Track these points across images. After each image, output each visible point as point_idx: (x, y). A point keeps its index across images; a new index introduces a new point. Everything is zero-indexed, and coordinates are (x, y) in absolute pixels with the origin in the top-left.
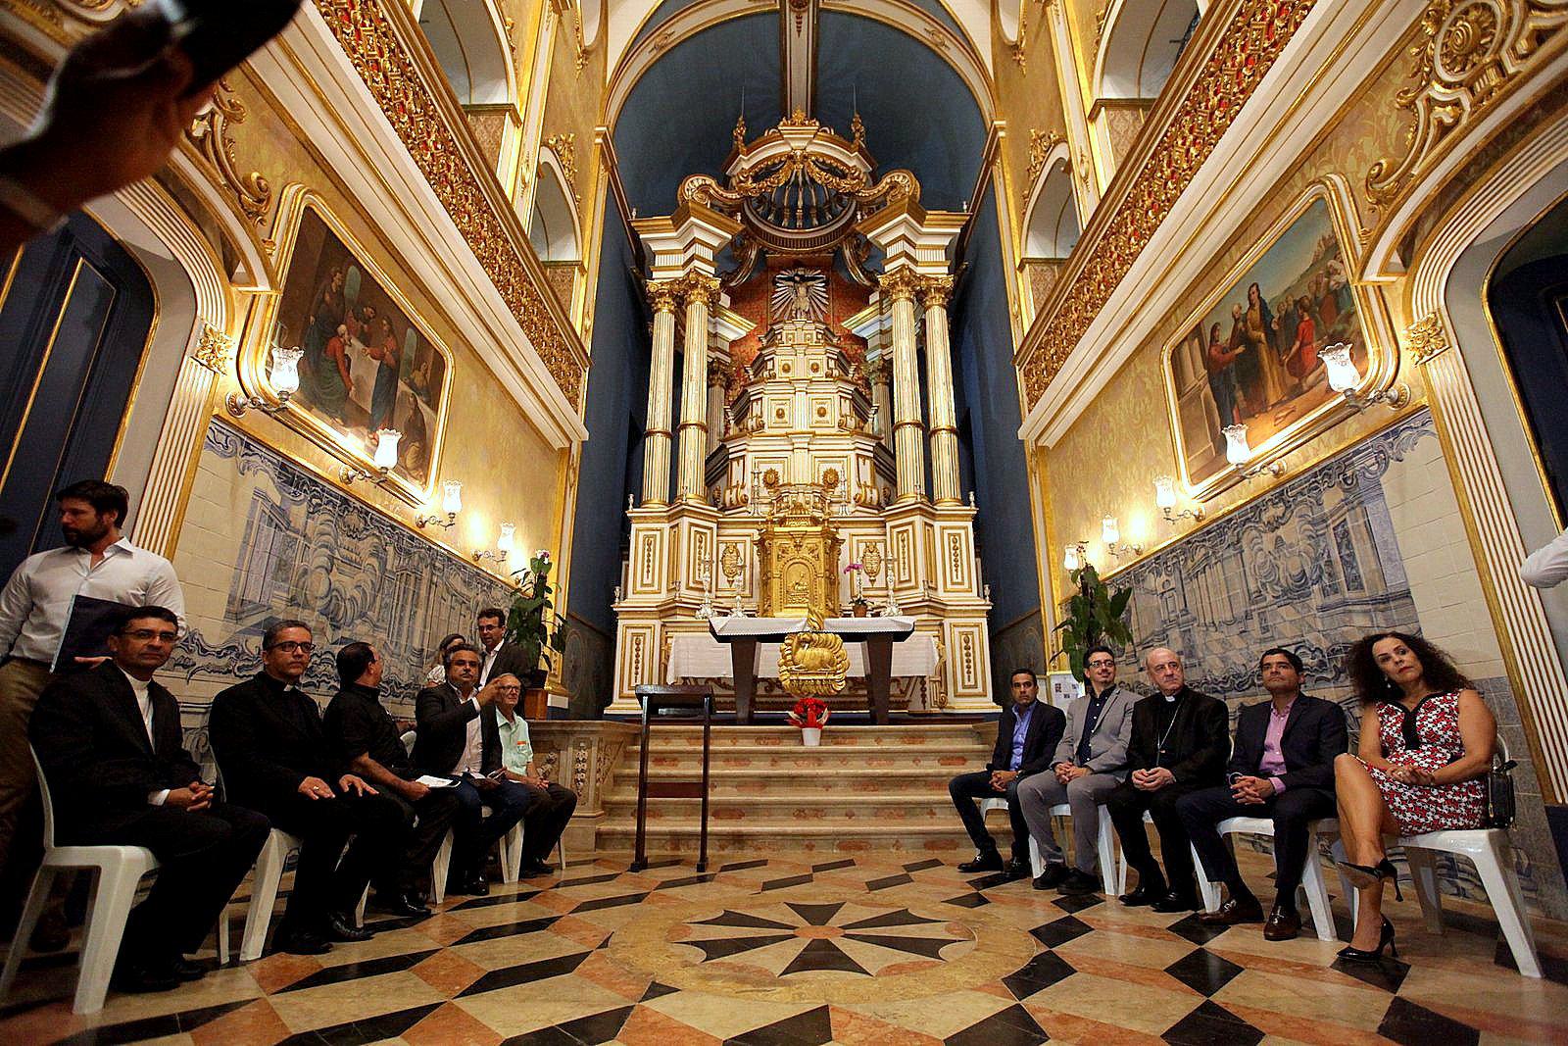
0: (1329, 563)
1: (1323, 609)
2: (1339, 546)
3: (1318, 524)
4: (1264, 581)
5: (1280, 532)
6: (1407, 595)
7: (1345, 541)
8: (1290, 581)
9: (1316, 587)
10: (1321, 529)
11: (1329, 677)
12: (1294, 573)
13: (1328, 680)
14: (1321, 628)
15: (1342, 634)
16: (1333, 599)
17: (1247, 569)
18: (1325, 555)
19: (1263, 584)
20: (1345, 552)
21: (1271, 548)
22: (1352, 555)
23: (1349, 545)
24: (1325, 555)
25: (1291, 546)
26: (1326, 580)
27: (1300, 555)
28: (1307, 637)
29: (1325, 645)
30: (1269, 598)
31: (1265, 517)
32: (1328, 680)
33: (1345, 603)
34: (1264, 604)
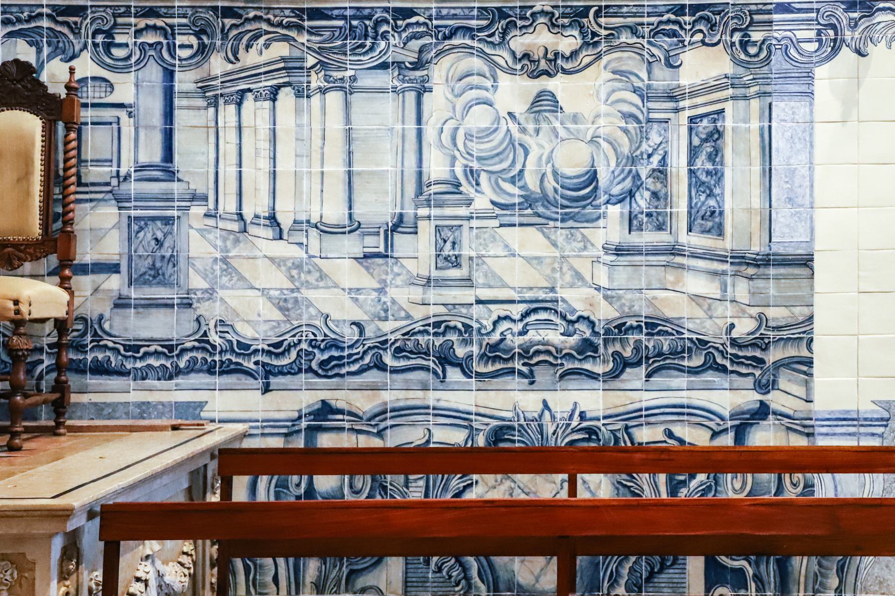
0: (661, 173)
1: (619, 251)
2: (693, 153)
3: (658, 98)
4: (475, 165)
5: (556, 84)
6: (806, 262)
7: (708, 148)
8: (550, 183)
9: (614, 211)
10: (660, 109)
11: (599, 369)
12: (569, 171)
13: (592, 376)
14: (604, 282)
15: (650, 303)
16: (649, 238)
17: (430, 133)
18: (656, 159)
19: (472, 174)
20: (701, 163)
21: (520, 109)
22: (717, 175)
23: (715, 155)
24: (656, 159)
25: (575, 119)
26: (642, 201)
27: (593, 141)
28: (561, 293)
29: (604, 313)
30: (481, 203)
31: (519, 42)
32: (592, 376)
33: (674, 250)
34: (463, 211)
